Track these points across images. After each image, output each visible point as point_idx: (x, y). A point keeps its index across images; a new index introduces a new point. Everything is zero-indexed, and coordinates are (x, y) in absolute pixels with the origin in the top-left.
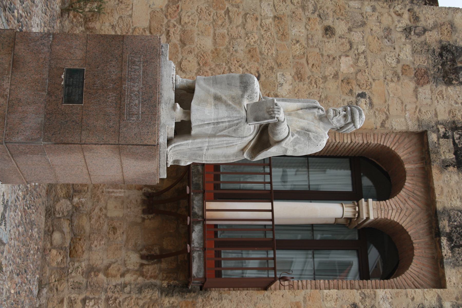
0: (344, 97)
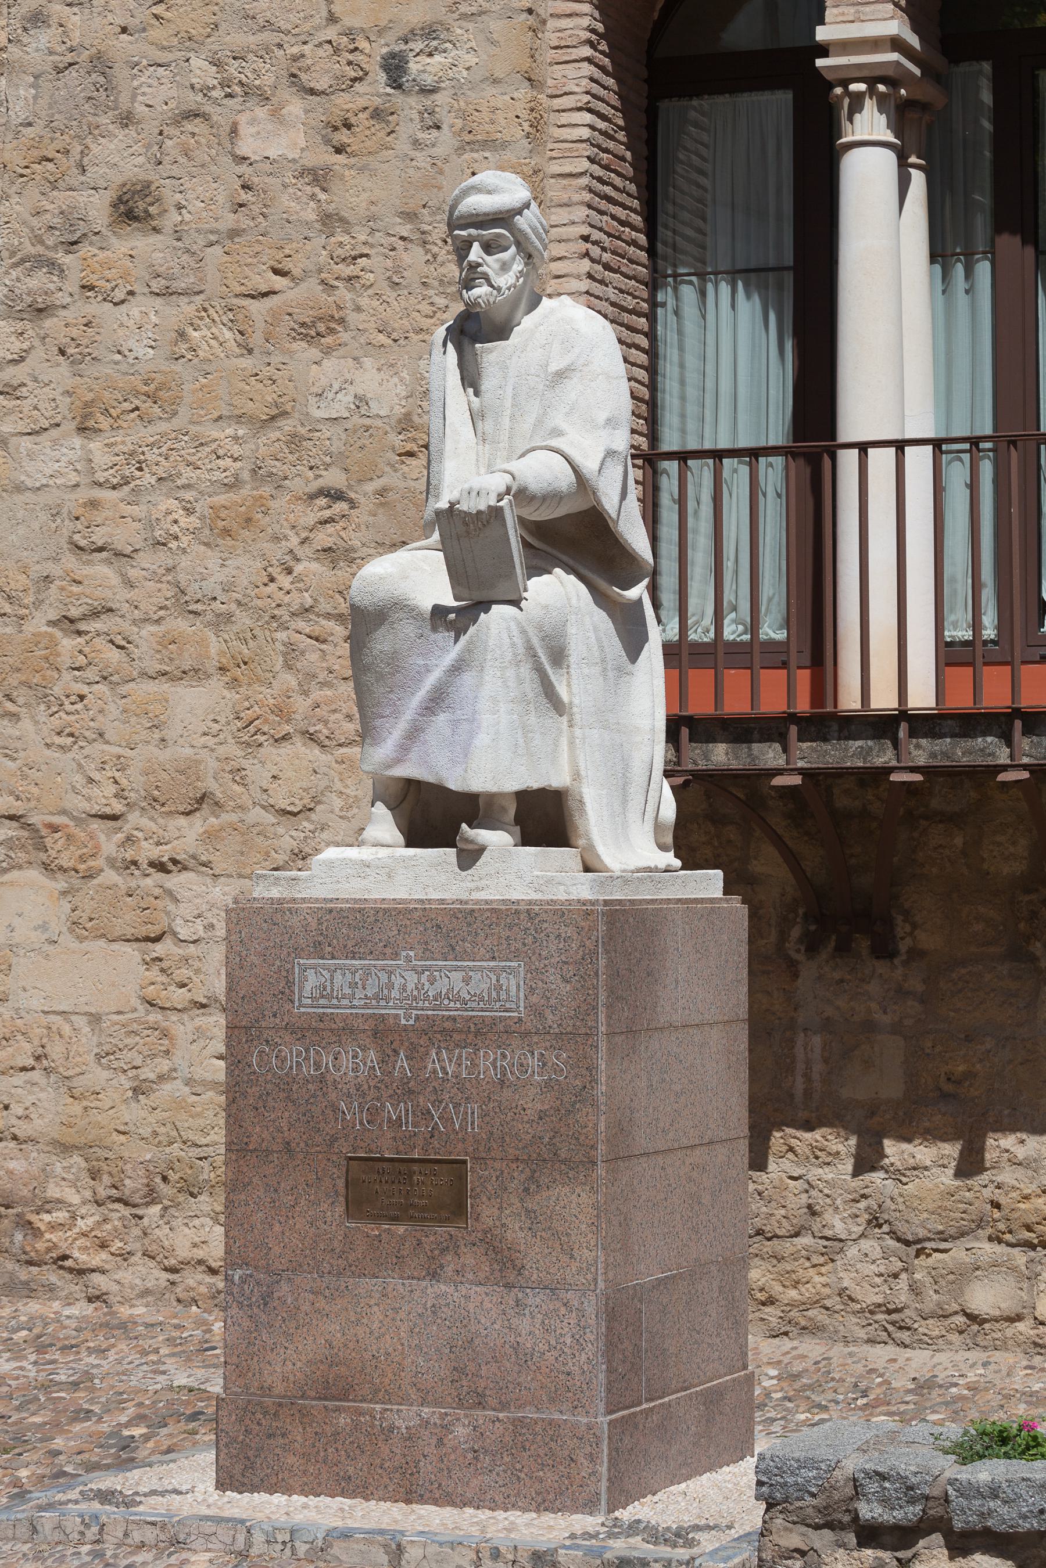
0: (403, 146)
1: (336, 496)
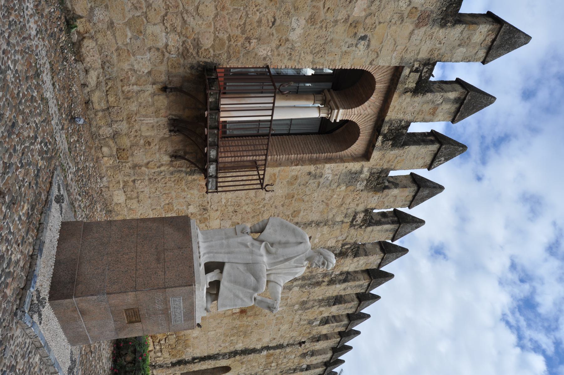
1: (273, 23)
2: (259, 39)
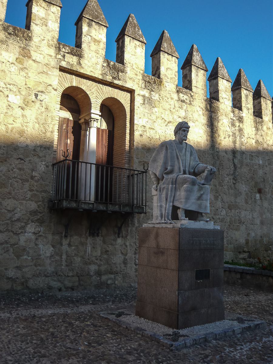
2: (33, 170)
